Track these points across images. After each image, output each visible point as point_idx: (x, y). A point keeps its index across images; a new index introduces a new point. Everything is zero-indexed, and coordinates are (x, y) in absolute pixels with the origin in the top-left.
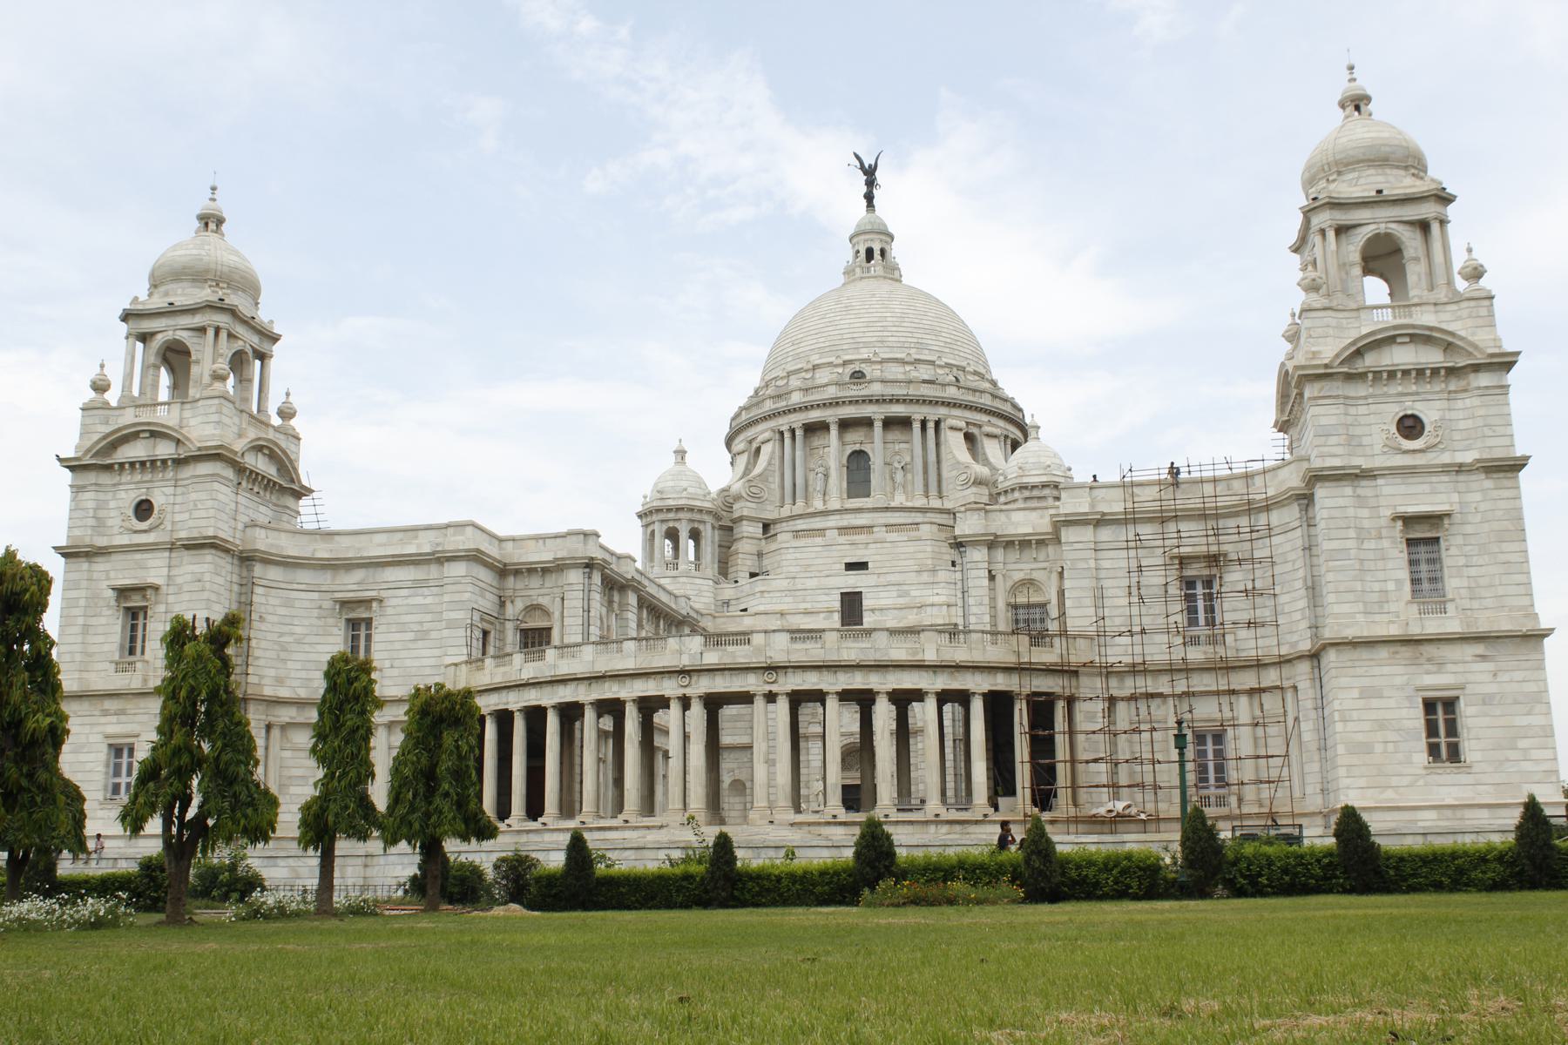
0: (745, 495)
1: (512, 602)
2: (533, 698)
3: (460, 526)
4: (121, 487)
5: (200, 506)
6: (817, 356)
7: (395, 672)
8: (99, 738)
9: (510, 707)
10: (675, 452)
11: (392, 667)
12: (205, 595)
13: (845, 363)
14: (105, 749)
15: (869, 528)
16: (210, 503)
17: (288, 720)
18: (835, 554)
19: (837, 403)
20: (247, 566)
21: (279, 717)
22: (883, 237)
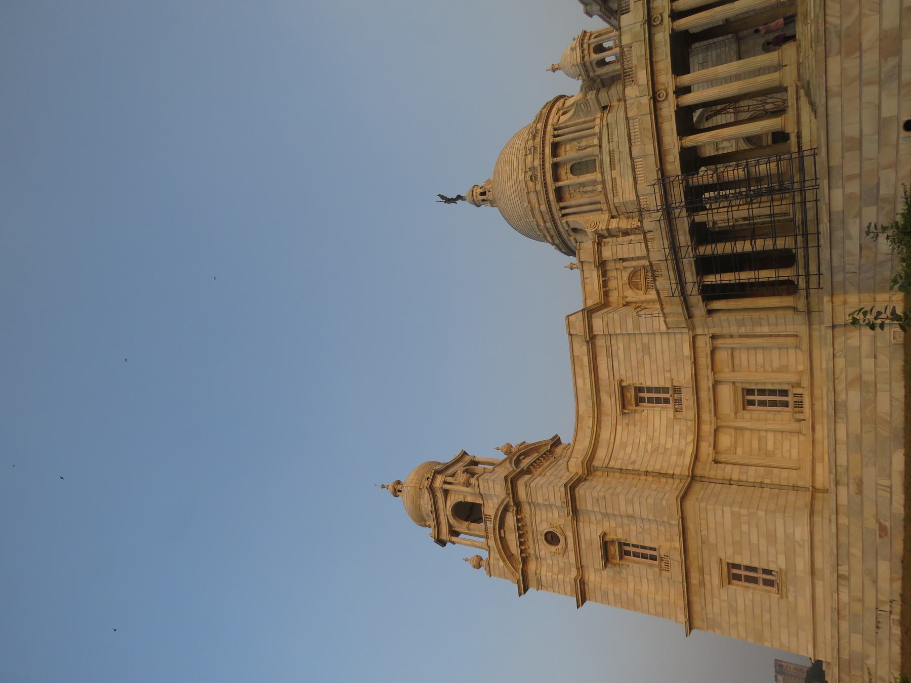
0: (595, 229)
1: (627, 297)
2: (684, 238)
3: (569, 325)
4: (538, 554)
5: (547, 497)
6: (525, 204)
8: (723, 592)
10: (572, 269)
11: (670, 371)
15: (611, 153)
16: (545, 490)
17: (712, 448)
18: (626, 170)
19: (545, 184)
20: (595, 471)
22: (475, 189)
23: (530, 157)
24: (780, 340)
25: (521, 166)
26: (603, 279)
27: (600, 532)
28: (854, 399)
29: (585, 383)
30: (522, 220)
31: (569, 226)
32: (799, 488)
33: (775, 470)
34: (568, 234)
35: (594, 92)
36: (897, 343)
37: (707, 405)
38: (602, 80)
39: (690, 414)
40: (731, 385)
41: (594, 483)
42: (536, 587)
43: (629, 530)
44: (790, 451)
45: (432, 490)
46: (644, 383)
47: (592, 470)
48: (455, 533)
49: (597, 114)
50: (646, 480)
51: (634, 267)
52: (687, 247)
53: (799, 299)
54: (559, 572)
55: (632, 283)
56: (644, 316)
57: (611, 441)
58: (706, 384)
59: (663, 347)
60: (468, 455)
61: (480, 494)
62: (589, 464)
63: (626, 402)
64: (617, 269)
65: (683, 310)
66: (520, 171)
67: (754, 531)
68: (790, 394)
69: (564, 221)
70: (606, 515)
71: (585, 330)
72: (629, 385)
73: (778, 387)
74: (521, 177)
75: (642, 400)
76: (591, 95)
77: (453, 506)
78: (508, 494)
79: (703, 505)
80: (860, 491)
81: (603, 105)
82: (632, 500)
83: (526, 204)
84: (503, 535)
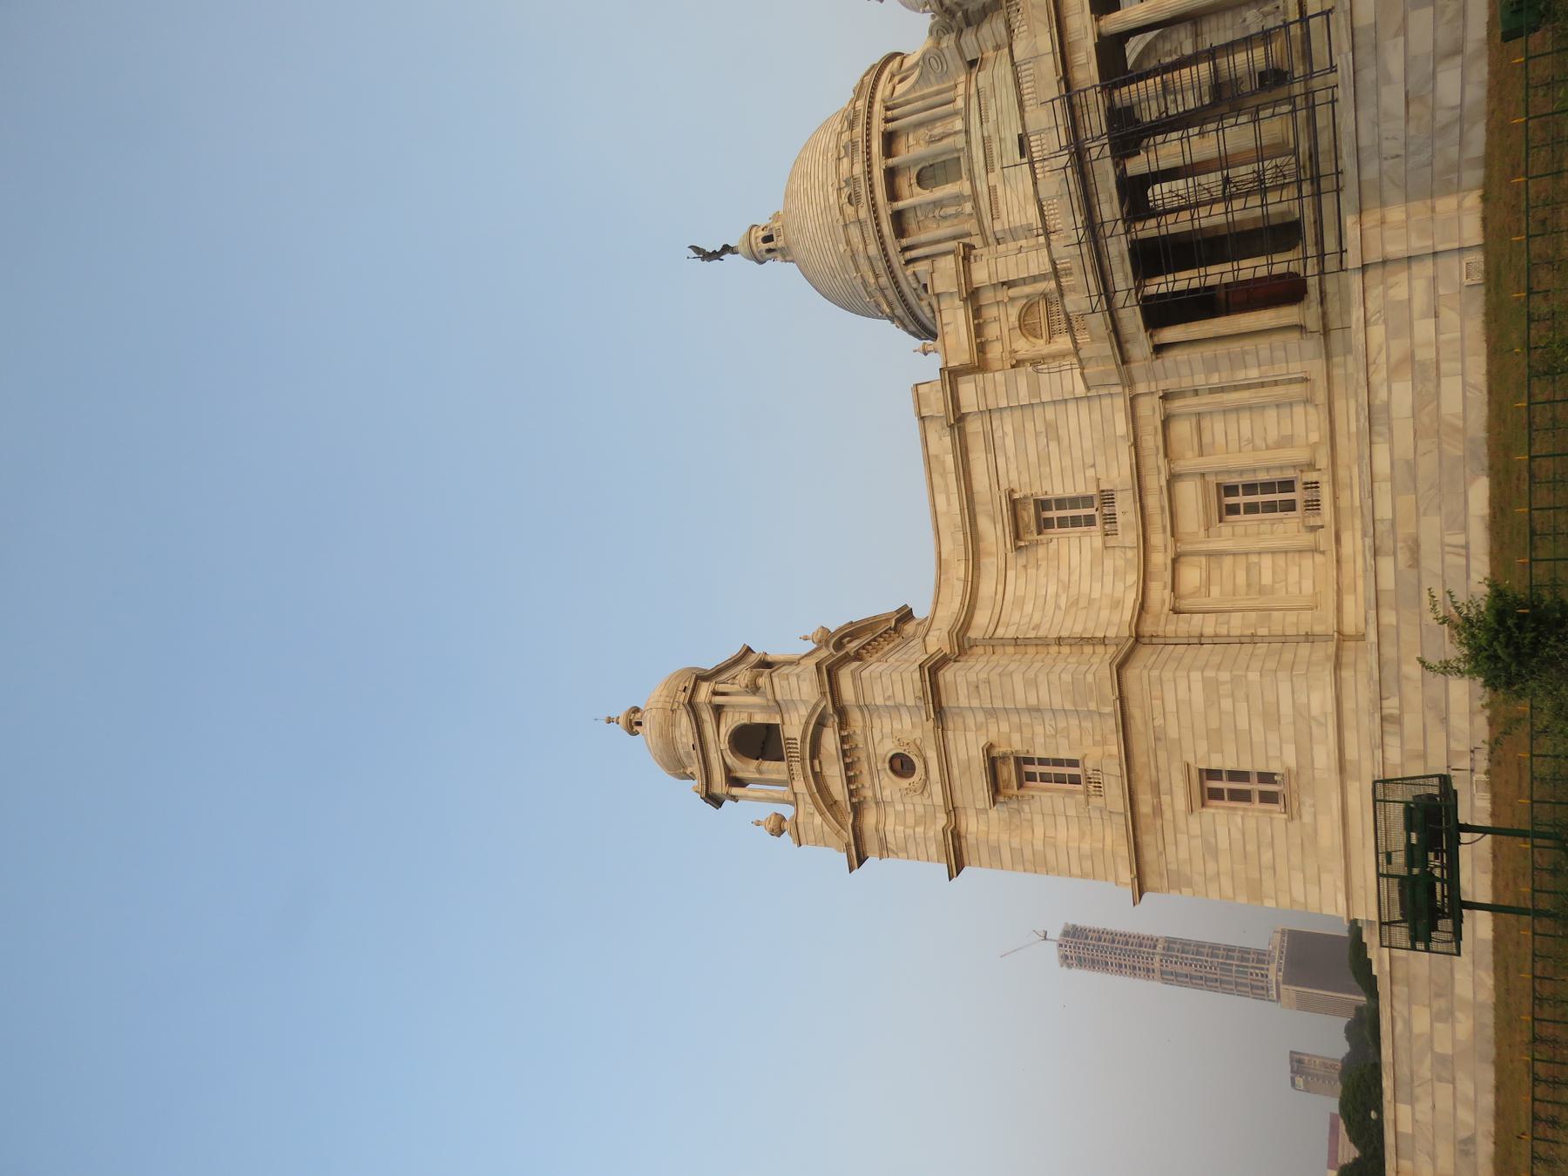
1: (1016, 352)
4: (879, 796)
5: (890, 693)
6: (841, 247)
7: (1100, 461)
8: (1194, 822)
9: (1125, 247)
10: (926, 354)
11: (1094, 466)
12: (994, 677)
13: (841, 210)
14: (1208, 812)
15: (986, 142)
17: (1168, 591)
19: (873, 205)
20: (971, 647)
21: (1163, 602)
23: (846, 162)
24: (1279, 391)
25: (832, 178)
26: (976, 322)
27: (983, 742)
28: (1401, 396)
29: (950, 504)
30: (838, 277)
31: (919, 282)
32: (1315, 637)
33: (1275, 614)
34: (918, 296)
35: (953, 35)
36: (1473, 283)
37: (1158, 520)
38: (965, 13)
39: (1129, 536)
40: (1198, 481)
41: (972, 662)
42: (878, 855)
43: (1033, 734)
44: (1300, 582)
45: (692, 707)
46: (1050, 492)
47: (967, 646)
48: (740, 783)
49: (959, 77)
50: (1059, 653)
51: (1027, 296)
52: (1113, 223)
53: (1308, 309)
54: (916, 824)
55: (1025, 326)
56: (1046, 371)
57: (997, 597)
58: (1155, 482)
59: (1078, 423)
60: (753, 652)
61: (777, 702)
62: (960, 635)
63: (1021, 525)
64: (998, 302)
65: (1112, 348)
66: (830, 188)
67: (1242, 707)
68: (1298, 486)
69: (909, 272)
70: (992, 713)
71: (946, 405)
72: (1025, 497)
73: (1276, 476)
74: (833, 199)
75: (1048, 523)
76: (948, 41)
77: (730, 736)
78: (823, 694)
79: (1155, 673)
80: (1415, 562)
81: (969, 59)
82: (1036, 676)
83: (842, 247)
84: (817, 769)
